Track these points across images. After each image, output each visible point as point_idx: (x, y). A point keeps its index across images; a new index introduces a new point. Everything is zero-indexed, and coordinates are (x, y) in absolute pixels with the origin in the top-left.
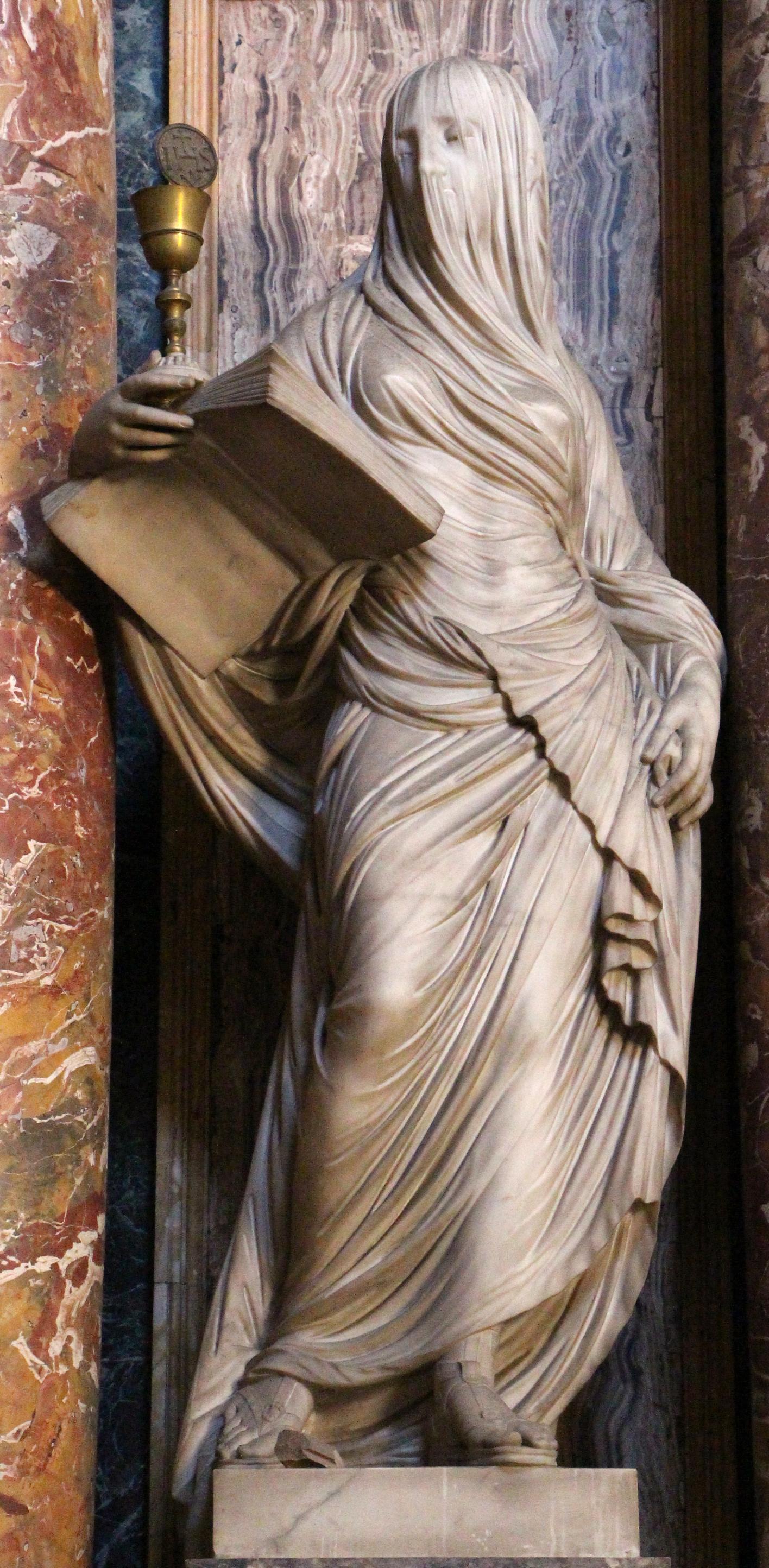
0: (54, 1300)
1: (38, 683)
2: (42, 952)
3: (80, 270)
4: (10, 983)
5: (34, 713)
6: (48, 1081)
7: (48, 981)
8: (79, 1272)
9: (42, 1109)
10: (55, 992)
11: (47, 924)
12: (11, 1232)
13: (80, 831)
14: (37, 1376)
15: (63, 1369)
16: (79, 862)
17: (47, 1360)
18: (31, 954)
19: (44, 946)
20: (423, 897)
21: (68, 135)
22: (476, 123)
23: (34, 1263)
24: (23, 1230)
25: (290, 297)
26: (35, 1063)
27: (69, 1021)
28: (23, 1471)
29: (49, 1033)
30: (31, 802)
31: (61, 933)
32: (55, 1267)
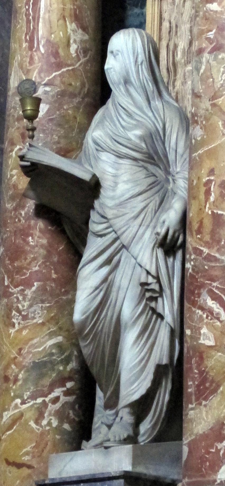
0: (43, 409)
1: (38, 237)
2: (39, 313)
3: (58, 112)
4: (29, 324)
5: (37, 246)
6: (40, 349)
7: (41, 321)
8: (57, 399)
9: (38, 358)
10: (43, 324)
11: (40, 305)
12: (28, 393)
13: (54, 276)
14: (37, 431)
15: (48, 428)
16: (53, 285)
17: (41, 426)
18: (35, 315)
19: (40, 312)
20: (86, 289)
21: (54, 74)
22: (118, 51)
23: (36, 400)
24: (32, 392)
25: (174, 87)
26: (36, 345)
27: (48, 332)
28: (33, 457)
29: (41, 336)
30: (36, 271)
31: (46, 306)
32: (44, 401)
